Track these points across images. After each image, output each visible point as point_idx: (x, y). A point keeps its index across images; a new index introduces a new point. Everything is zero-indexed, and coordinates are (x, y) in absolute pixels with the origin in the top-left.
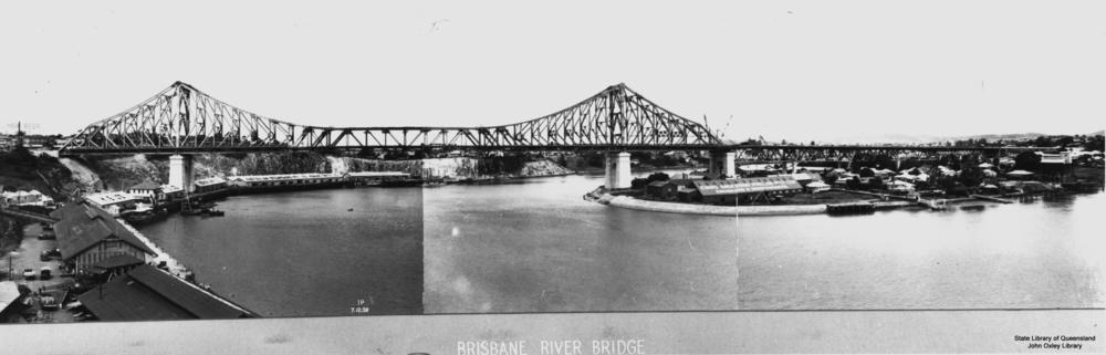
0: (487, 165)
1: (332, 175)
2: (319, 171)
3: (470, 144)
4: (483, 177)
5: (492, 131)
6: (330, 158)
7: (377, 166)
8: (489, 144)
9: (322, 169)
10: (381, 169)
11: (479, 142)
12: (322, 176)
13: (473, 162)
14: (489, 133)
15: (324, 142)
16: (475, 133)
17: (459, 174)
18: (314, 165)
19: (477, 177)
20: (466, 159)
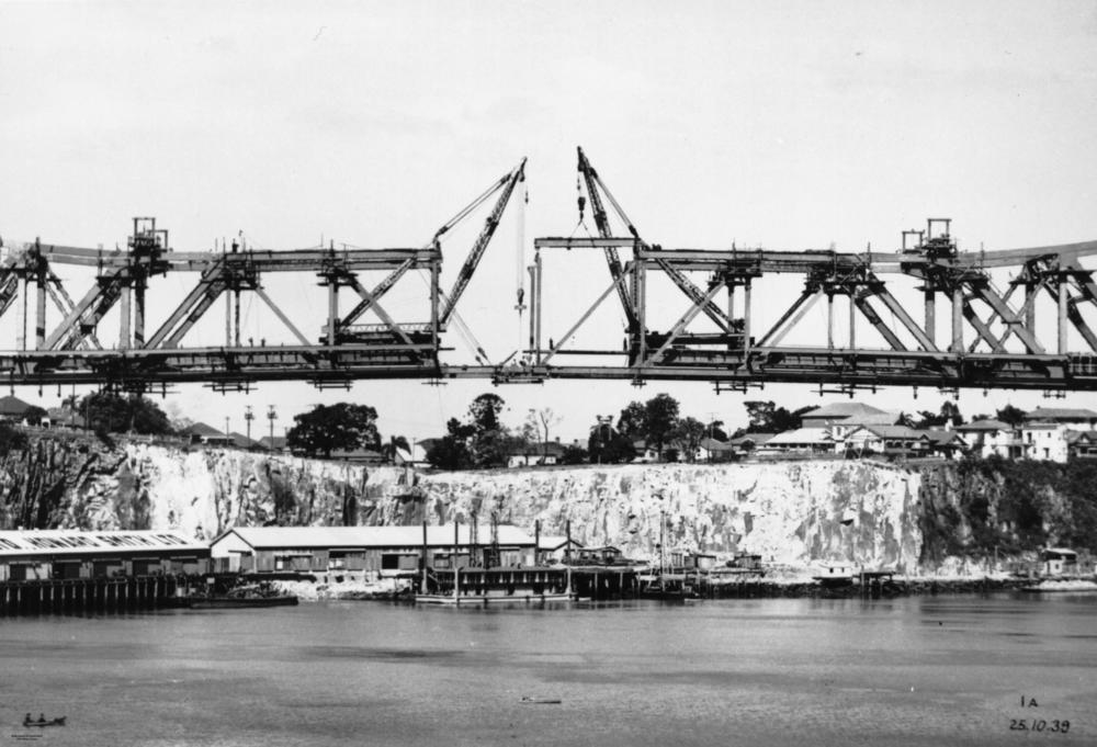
0: (977, 508)
1: (135, 541)
2: (85, 524)
3: (870, 340)
4: (951, 570)
5: (1000, 278)
6: (140, 451)
7: (386, 502)
8: (984, 349)
9: (105, 512)
10: (411, 505)
11: (929, 334)
12: (95, 542)
13: (897, 490)
14: (980, 285)
15: (110, 335)
16: (906, 289)
17: (815, 552)
18: (56, 495)
19: (912, 570)
20: (853, 468)
